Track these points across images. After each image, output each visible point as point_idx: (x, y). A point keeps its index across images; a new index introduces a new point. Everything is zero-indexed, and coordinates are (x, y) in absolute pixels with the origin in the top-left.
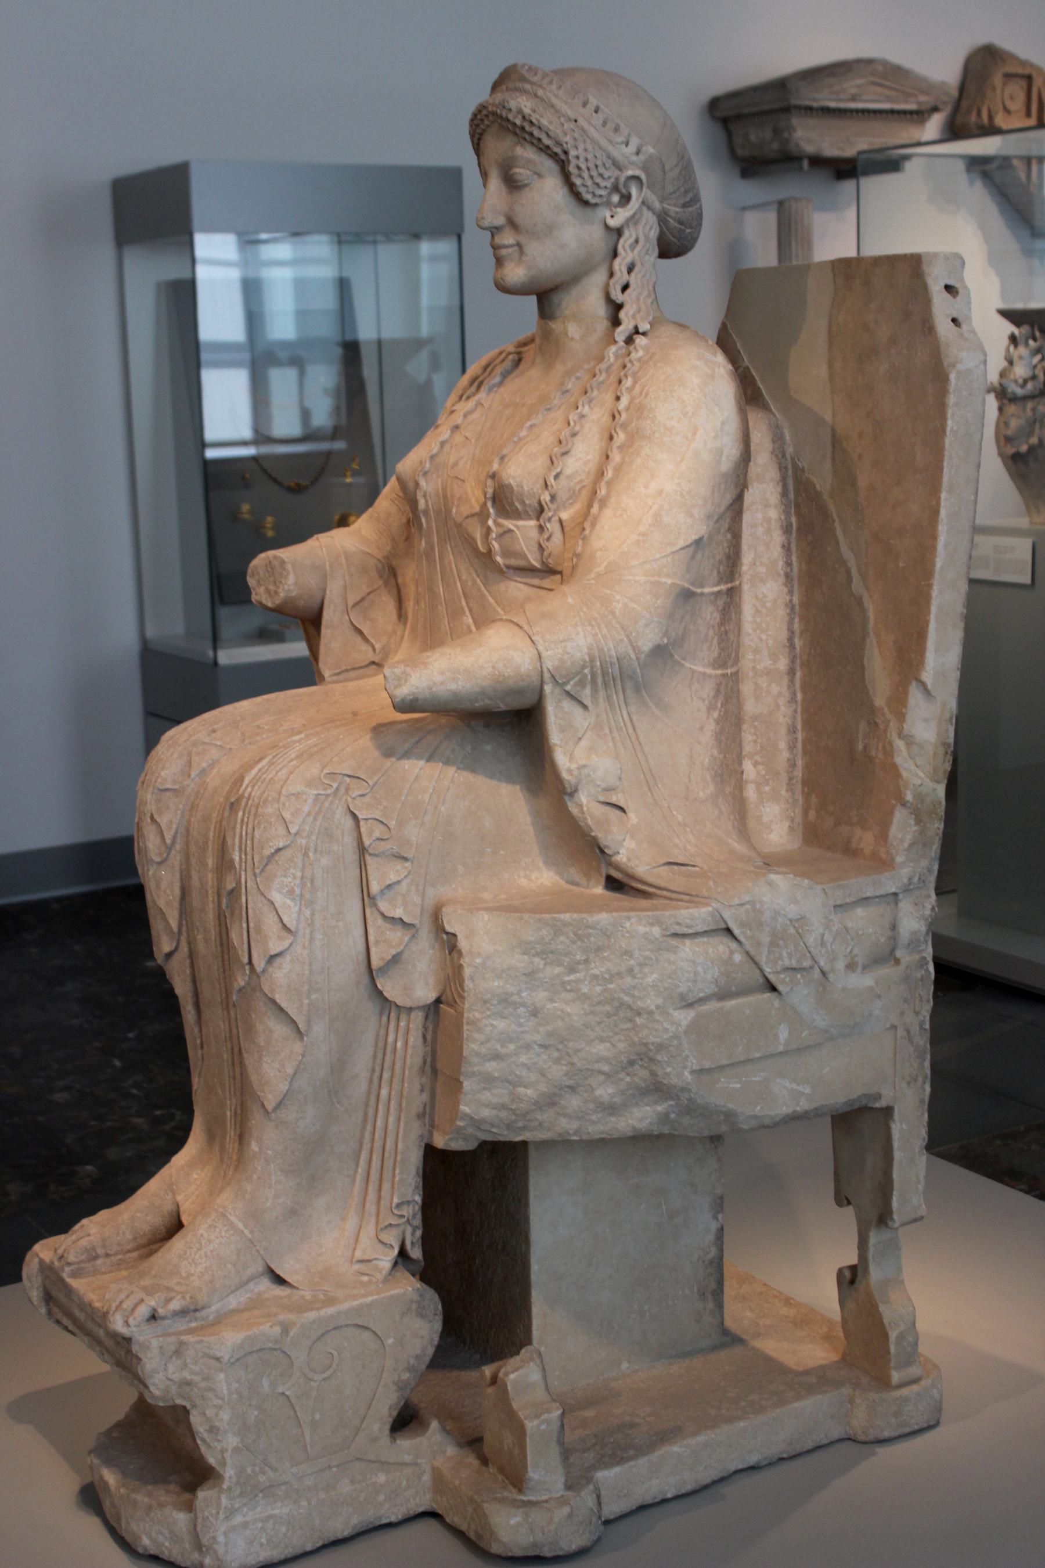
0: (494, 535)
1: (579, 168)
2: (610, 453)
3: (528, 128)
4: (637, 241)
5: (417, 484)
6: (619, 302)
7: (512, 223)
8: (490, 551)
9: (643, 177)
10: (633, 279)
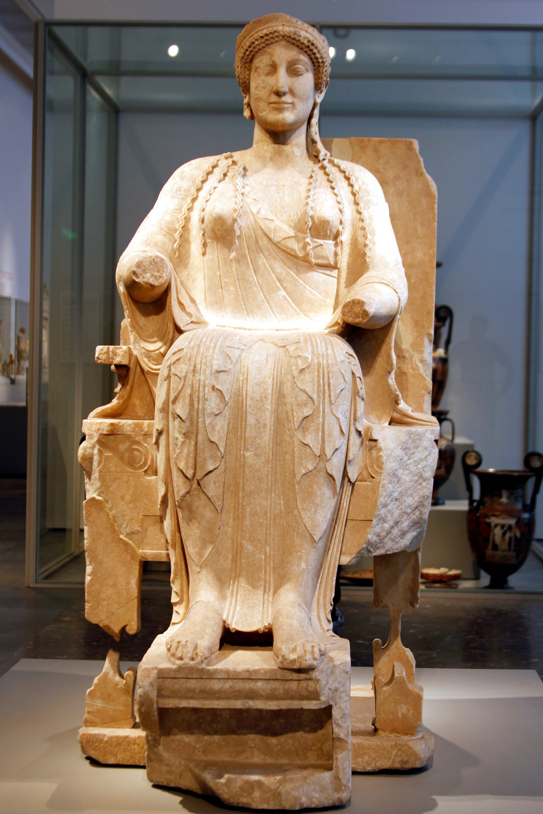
0: (311, 247)
2: (360, 211)
7: (292, 92)
8: (307, 255)
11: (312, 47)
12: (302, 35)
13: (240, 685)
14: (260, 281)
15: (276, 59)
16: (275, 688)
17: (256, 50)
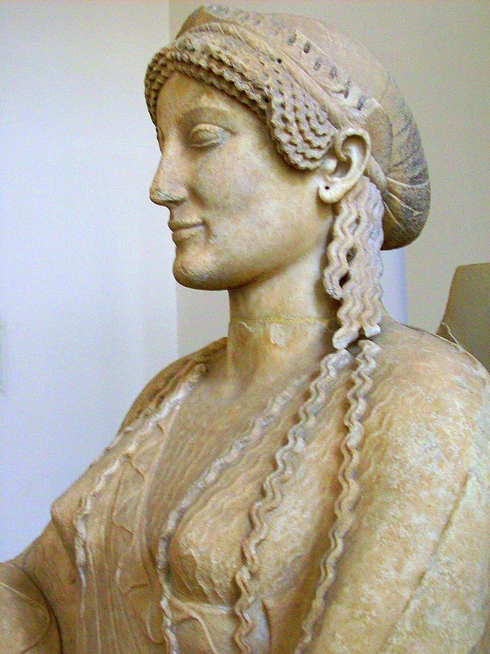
1: (285, 120)
3: (216, 70)
4: (358, 221)
5: (75, 531)
6: (337, 297)
7: (196, 196)
9: (367, 137)
10: (355, 270)
12: (198, 48)
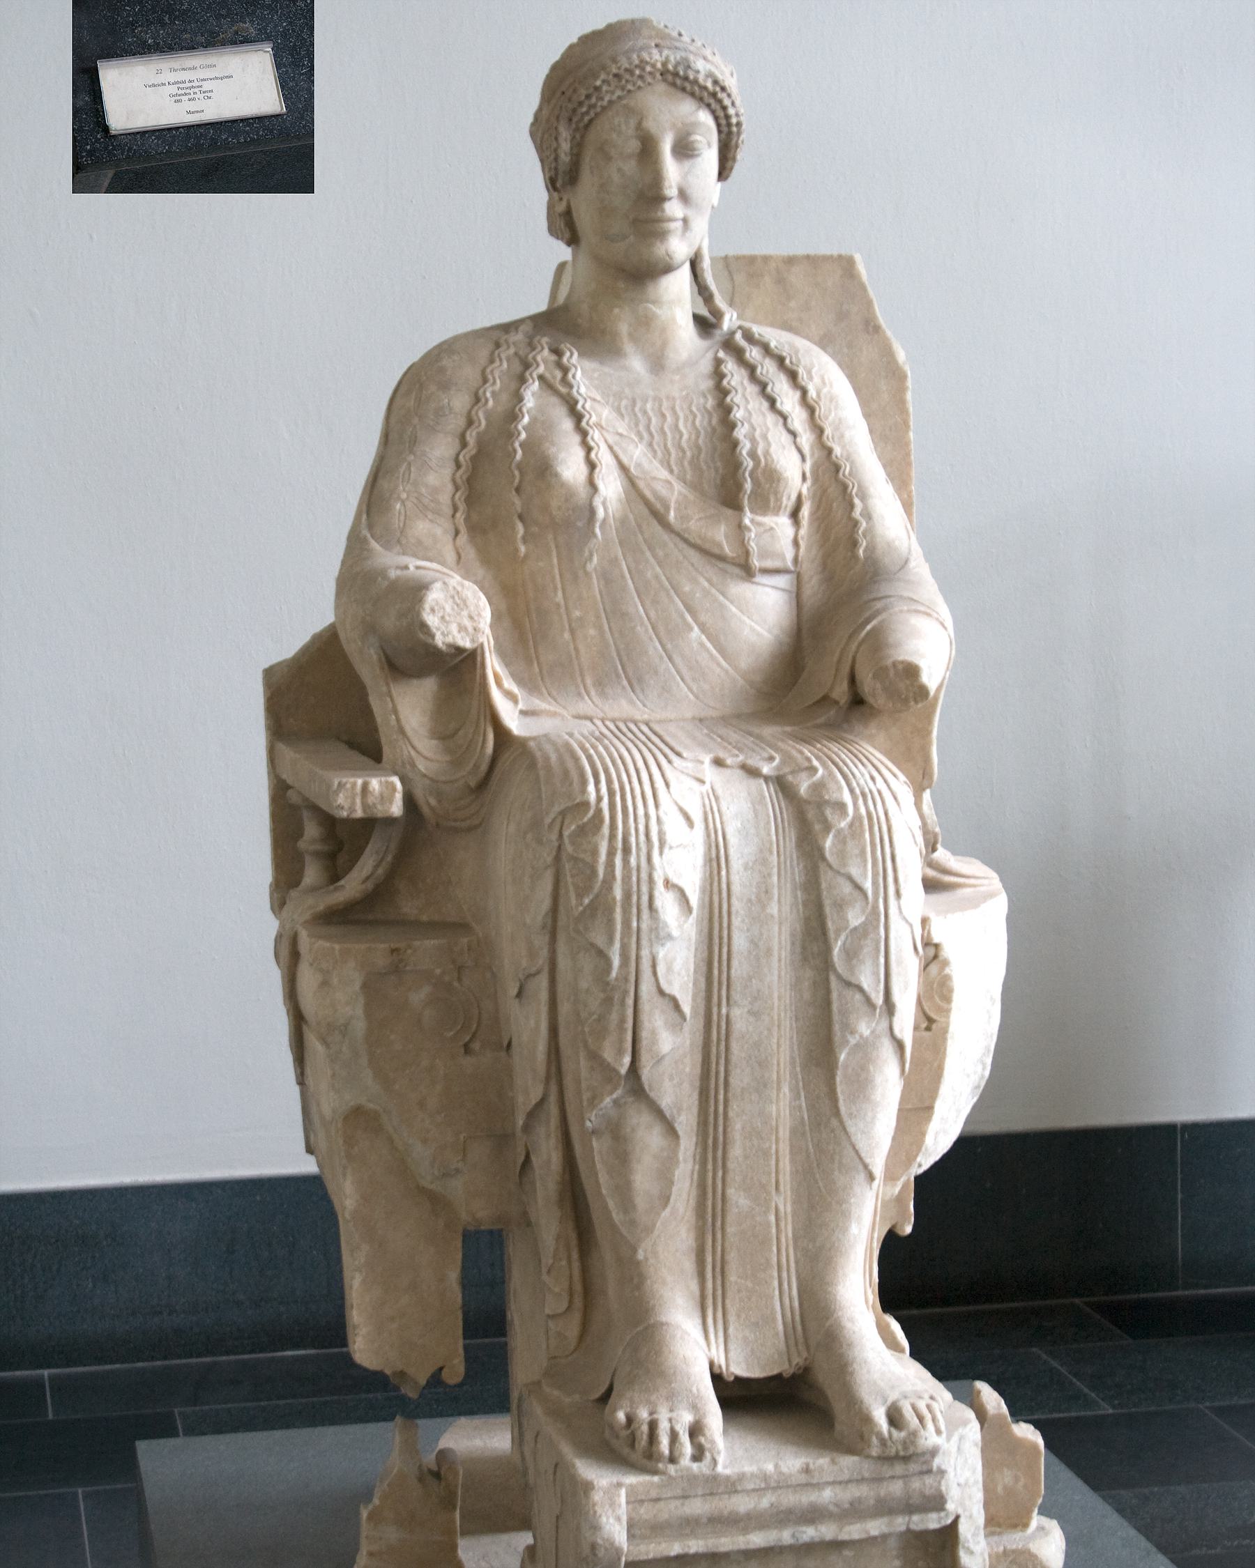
7: (684, 196)
11: (721, 95)
13: (790, 1499)
14: (652, 614)
15: (650, 124)
16: (860, 1498)
17: (605, 103)
